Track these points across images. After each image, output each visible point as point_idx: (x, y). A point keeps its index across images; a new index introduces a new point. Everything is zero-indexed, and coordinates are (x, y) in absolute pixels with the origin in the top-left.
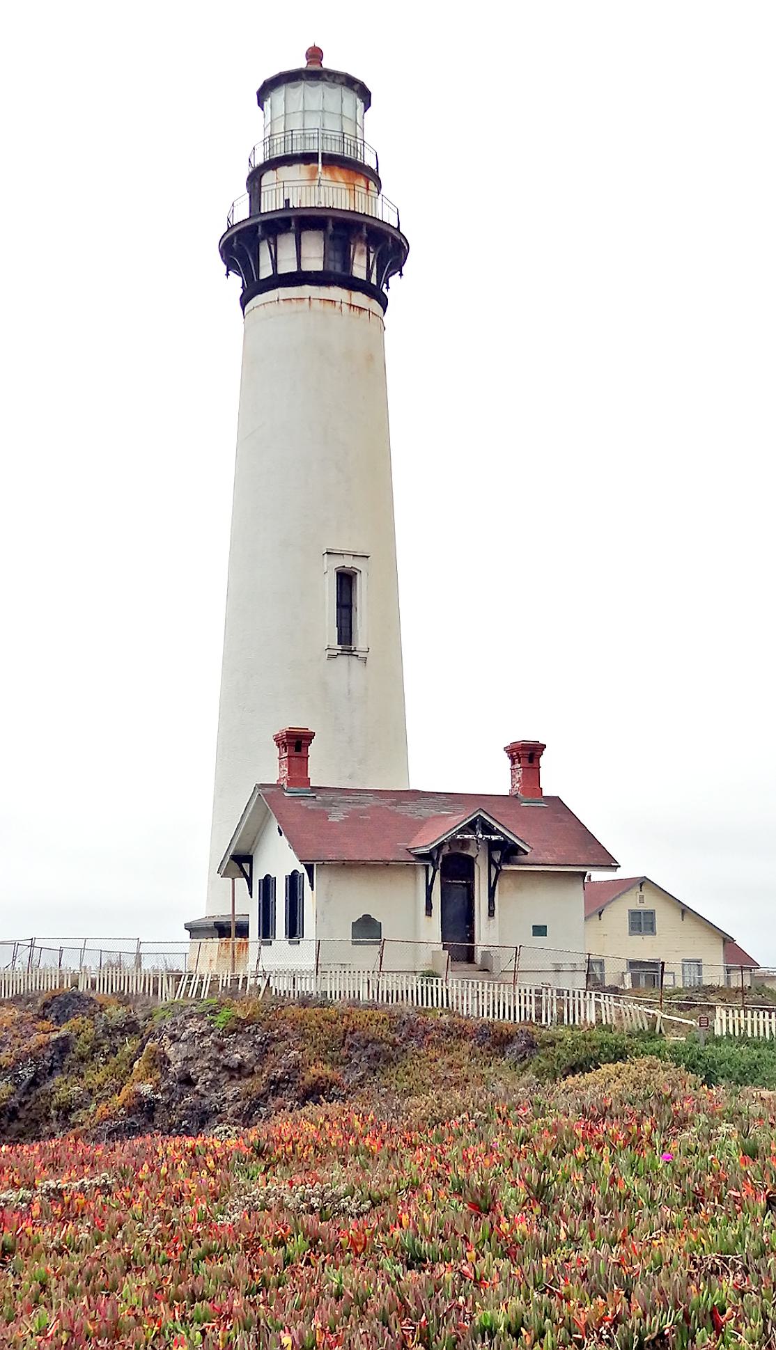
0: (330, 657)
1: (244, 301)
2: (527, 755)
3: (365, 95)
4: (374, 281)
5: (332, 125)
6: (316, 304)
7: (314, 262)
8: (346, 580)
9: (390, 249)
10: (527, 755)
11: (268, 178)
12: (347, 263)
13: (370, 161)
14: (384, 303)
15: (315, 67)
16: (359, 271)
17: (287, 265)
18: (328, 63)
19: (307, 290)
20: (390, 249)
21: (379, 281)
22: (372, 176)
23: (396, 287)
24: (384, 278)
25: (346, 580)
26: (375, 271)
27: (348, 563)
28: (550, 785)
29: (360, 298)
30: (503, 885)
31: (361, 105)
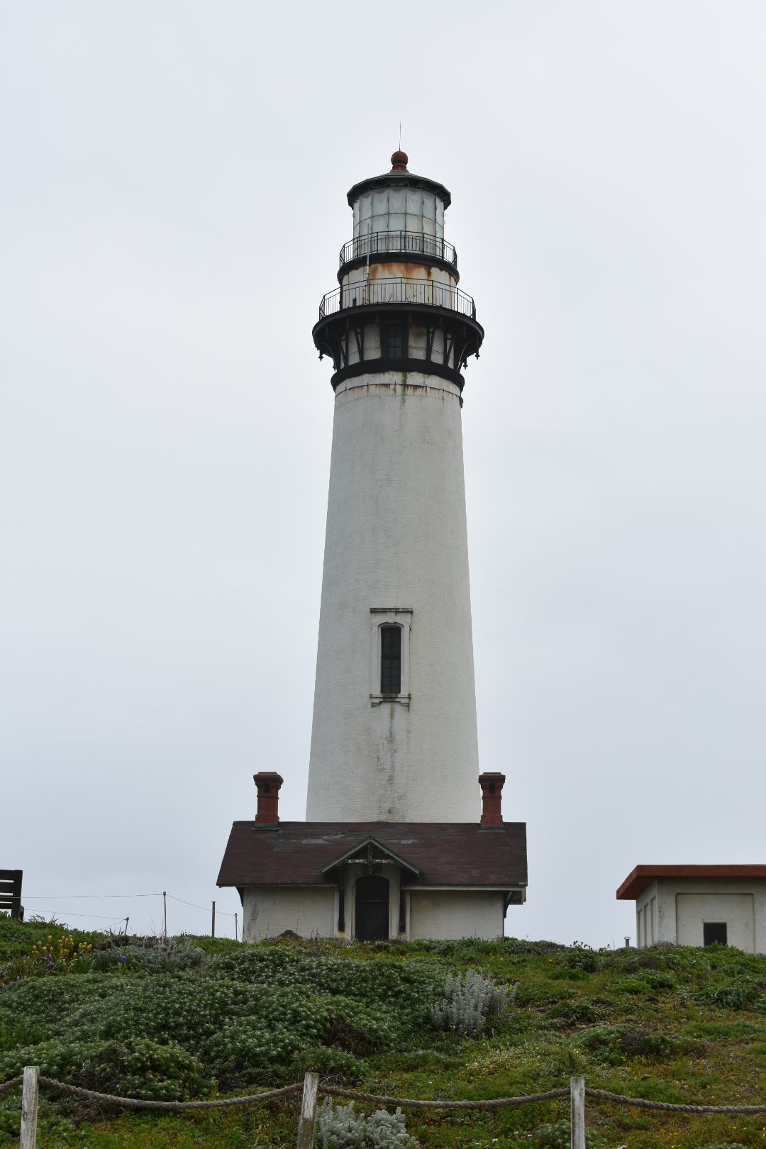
0: (374, 705)
3: (442, 195)
4: (451, 365)
5: (413, 226)
6: (372, 389)
9: (465, 335)
13: (448, 257)
14: (460, 382)
15: (400, 173)
18: (413, 169)
21: (456, 363)
22: (451, 270)
23: (472, 369)
24: (461, 359)
25: (391, 637)
26: (452, 355)
27: (390, 618)
31: (440, 204)
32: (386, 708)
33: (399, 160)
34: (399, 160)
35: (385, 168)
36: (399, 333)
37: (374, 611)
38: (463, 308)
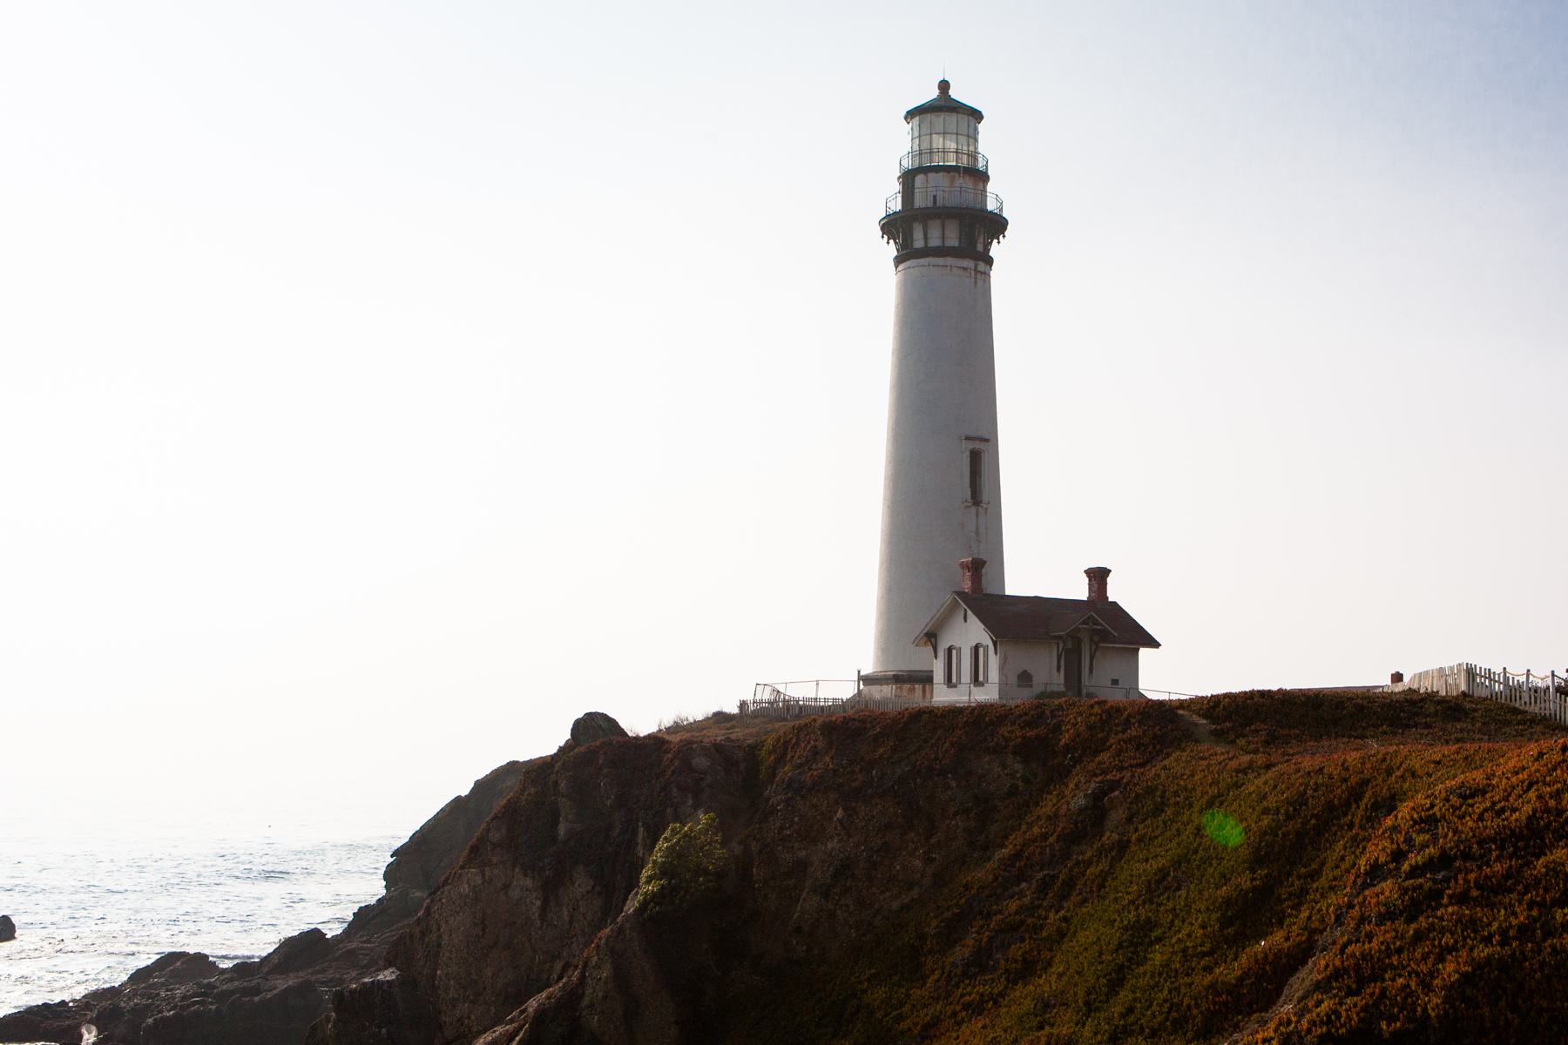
1: (898, 261)
2: (1098, 577)
7: (953, 241)
8: (975, 458)
10: (1098, 577)
11: (919, 179)
12: (973, 243)
16: (980, 248)
17: (935, 242)
19: (949, 261)
20: (997, 225)
22: (983, 177)
25: (975, 458)
27: (978, 445)
28: (1112, 595)
29: (982, 266)
30: (1098, 654)
32: (973, 509)
33: (944, 86)
34: (944, 86)
35: (934, 93)
36: (945, 224)
37: (968, 438)
38: (991, 206)
